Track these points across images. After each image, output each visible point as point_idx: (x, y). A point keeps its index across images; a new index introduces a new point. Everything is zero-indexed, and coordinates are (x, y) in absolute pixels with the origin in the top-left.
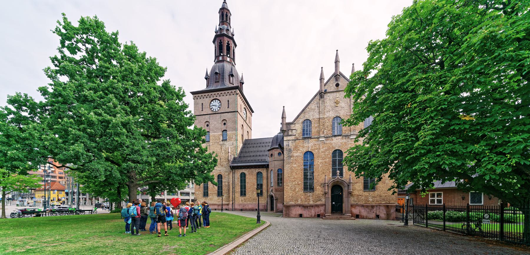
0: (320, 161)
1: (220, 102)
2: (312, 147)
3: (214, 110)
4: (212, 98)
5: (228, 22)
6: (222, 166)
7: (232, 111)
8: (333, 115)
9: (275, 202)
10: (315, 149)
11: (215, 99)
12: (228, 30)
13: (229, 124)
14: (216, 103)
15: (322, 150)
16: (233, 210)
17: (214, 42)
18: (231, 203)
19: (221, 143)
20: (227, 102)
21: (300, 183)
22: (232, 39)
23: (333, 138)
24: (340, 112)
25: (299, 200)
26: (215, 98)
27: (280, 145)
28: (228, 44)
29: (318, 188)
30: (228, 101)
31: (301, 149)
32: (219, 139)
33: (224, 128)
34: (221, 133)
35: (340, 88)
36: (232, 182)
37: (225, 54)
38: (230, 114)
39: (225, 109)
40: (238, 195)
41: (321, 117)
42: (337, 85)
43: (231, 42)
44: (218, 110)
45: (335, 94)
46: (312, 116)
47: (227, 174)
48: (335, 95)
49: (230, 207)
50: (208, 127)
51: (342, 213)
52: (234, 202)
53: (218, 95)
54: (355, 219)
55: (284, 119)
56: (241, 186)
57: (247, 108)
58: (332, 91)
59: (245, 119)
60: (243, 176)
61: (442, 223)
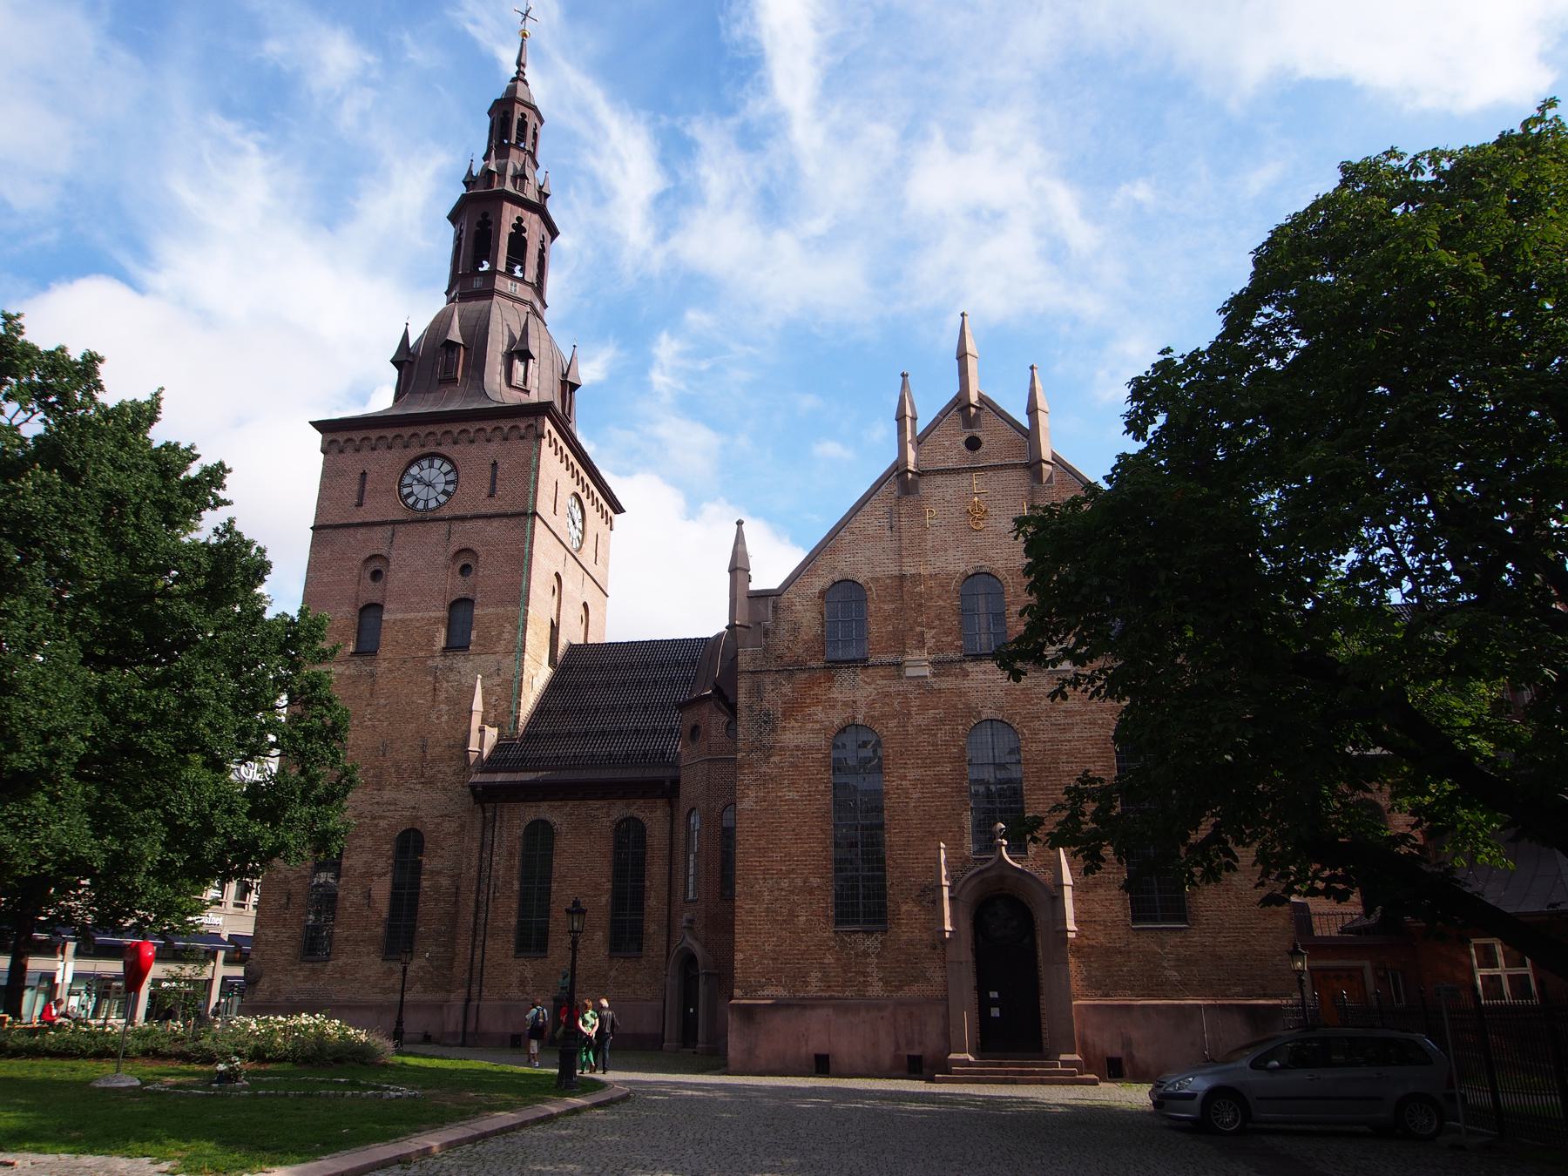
0: (912, 774)
1: (455, 469)
2: (871, 705)
3: (420, 505)
4: (415, 451)
5: (529, 147)
6: (429, 783)
7: (510, 510)
8: (962, 568)
9: (702, 989)
10: (883, 716)
11: (432, 456)
12: (524, 177)
13: (485, 570)
14: (436, 473)
15: (917, 720)
16: (463, 1044)
18: (458, 997)
19: (438, 661)
20: (488, 467)
21: (815, 881)
22: (540, 210)
23: (969, 666)
24: (991, 553)
25: (815, 976)
27: (718, 690)
28: (519, 228)
29: (909, 913)
30: (495, 464)
31: (821, 716)
32: (431, 641)
33: (460, 587)
34: (443, 614)
35: (985, 456)
36: (473, 873)
37: (502, 266)
38: (496, 523)
39: (473, 497)
40: (500, 948)
41: (909, 570)
42: (973, 444)
43: (532, 222)
44: (440, 505)
45: (963, 481)
46: (866, 568)
47: (450, 826)
48: (966, 483)
49: (453, 1021)
50: (379, 585)
51: (1040, 1049)
52: (475, 989)
54: (1094, 1083)
55: (740, 574)
56: (525, 898)
58: (950, 465)
60: (540, 838)
61: (1505, 1100)
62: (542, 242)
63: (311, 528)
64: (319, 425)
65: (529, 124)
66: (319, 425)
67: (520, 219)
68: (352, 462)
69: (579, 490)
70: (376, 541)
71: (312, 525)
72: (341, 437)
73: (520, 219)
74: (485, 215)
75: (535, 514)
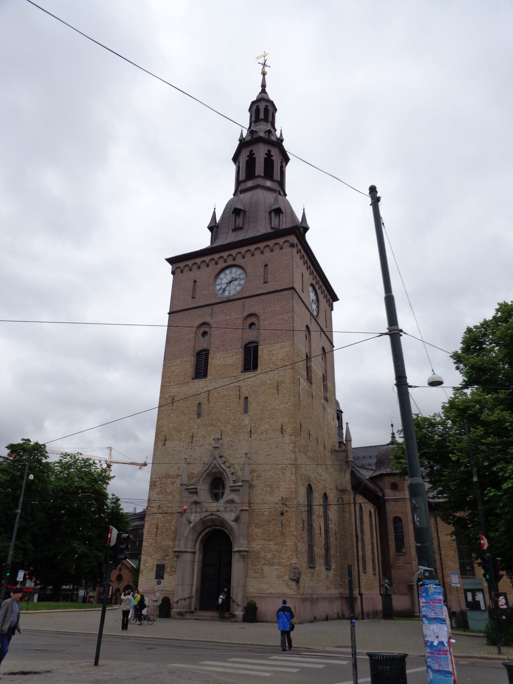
4: (222, 265)
17: (235, 159)
26: (230, 262)
28: (269, 155)
43: (275, 152)
53: (239, 257)
57: (320, 288)
59: (315, 313)
62: (281, 163)
63: (168, 313)
64: (171, 261)
65: (270, 110)
66: (171, 261)
67: (269, 151)
68: (188, 276)
69: (314, 282)
70: (204, 315)
71: (168, 312)
72: (182, 265)
73: (269, 151)
74: (251, 151)
75: (293, 288)
